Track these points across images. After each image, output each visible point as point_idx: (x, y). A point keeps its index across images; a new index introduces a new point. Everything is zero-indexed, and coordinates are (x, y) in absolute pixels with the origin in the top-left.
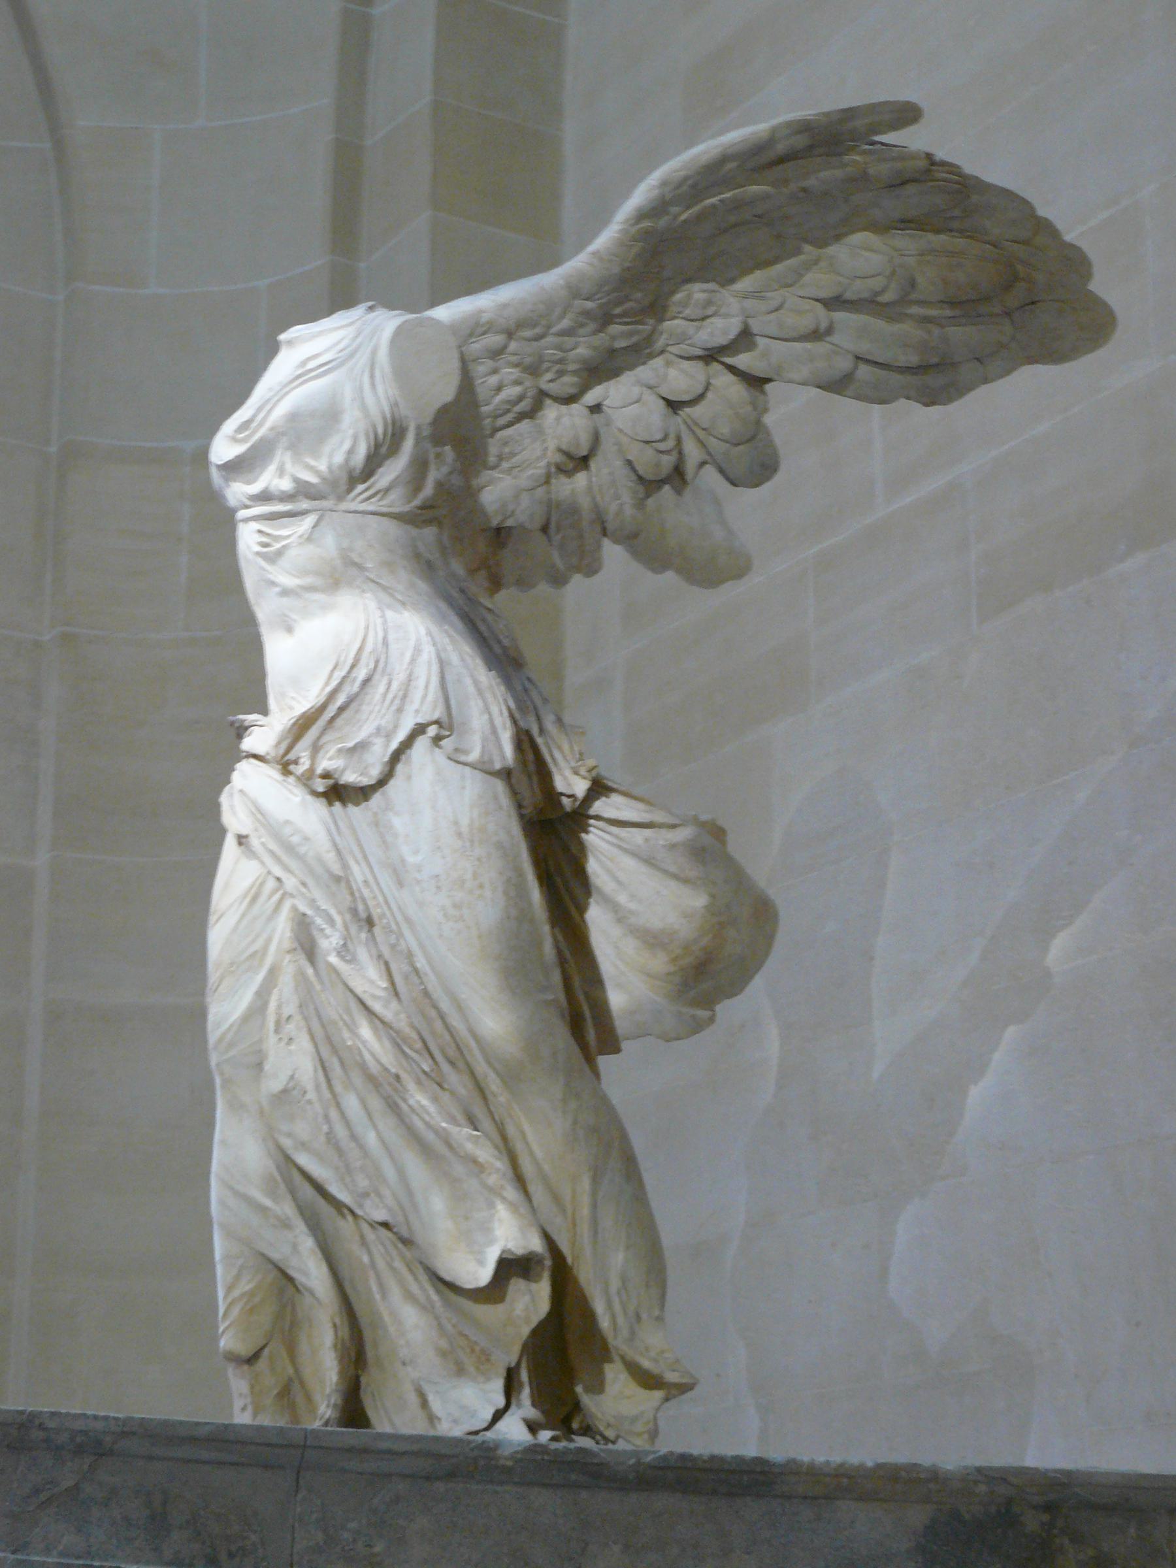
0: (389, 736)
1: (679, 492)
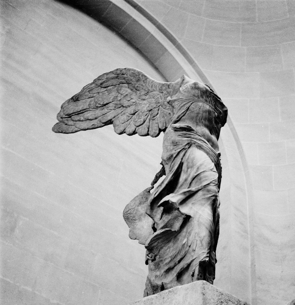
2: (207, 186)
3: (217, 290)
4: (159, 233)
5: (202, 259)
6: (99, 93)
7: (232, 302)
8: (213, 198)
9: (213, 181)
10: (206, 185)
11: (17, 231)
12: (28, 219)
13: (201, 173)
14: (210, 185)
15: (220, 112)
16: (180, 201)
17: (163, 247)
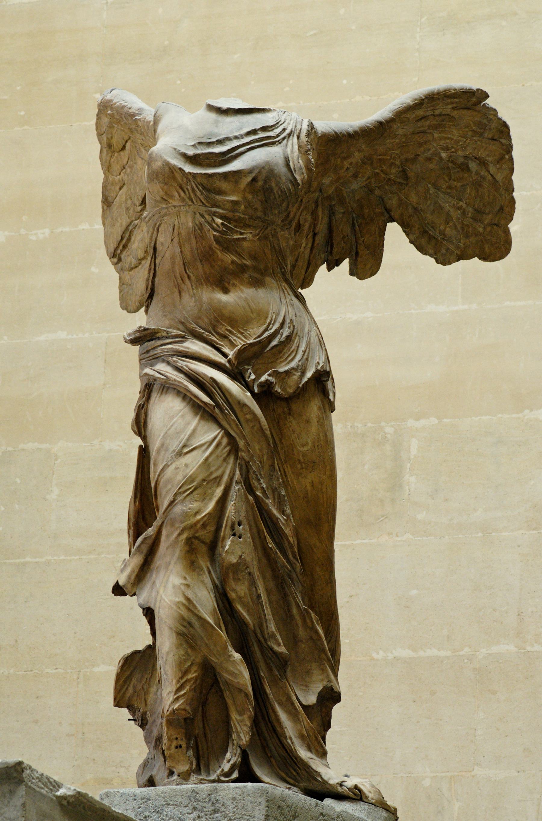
0: (303, 373)
1: (330, 269)
2: (170, 508)
3: (135, 796)
4: (119, 671)
5: (168, 710)
6: (124, 168)
7: (173, 805)
8: (184, 536)
9: (179, 488)
10: (167, 509)
11: (411, 480)
12: (434, 421)
13: (159, 475)
14: (176, 501)
15: (232, 202)
16: (133, 578)
17: (147, 690)
